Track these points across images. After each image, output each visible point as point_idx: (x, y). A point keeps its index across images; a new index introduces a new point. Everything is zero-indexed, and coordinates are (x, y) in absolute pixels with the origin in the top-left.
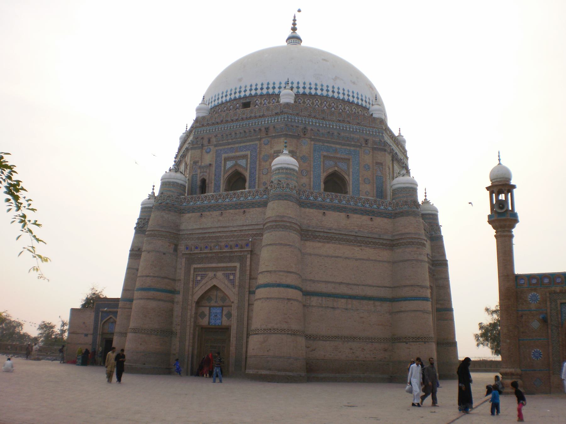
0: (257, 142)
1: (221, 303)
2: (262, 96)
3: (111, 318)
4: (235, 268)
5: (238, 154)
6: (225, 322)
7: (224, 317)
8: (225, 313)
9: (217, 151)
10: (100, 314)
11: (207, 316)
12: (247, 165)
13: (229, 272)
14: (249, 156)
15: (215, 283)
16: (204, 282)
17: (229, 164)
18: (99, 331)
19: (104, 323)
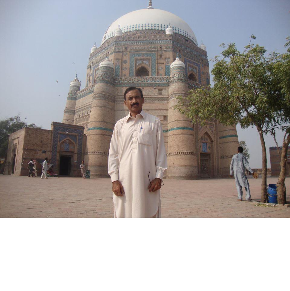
0: (200, 64)
1: (206, 141)
2: (191, 40)
3: (68, 139)
4: (214, 124)
5: (194, 66)
6: (209, 151)
7: (208, 148)
8: (208, 146)
9: (185, 59)
10: (59, 136)
11: (202, 147)
12: (197, 73)
13: (211, 126)
14: (198, 69)
15: (206, 131)
16: (202, 129)
17: (190, 69)
18: (58, 149)
19: (61, 143)
